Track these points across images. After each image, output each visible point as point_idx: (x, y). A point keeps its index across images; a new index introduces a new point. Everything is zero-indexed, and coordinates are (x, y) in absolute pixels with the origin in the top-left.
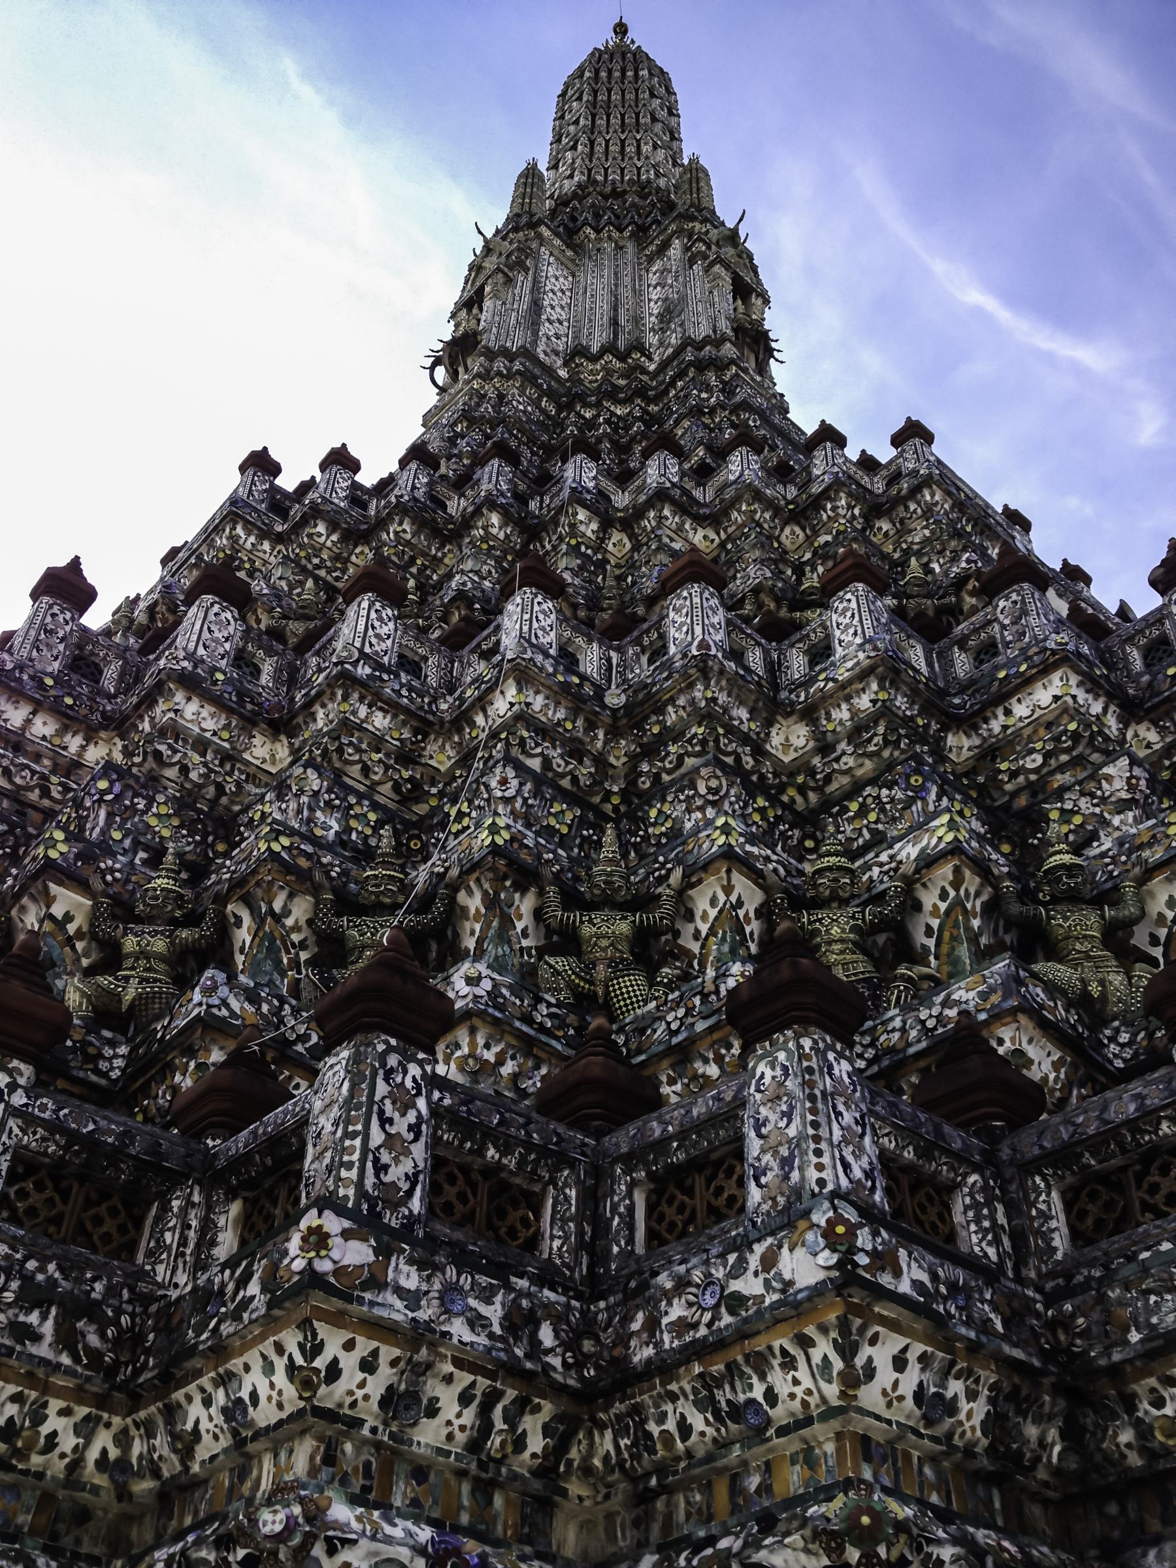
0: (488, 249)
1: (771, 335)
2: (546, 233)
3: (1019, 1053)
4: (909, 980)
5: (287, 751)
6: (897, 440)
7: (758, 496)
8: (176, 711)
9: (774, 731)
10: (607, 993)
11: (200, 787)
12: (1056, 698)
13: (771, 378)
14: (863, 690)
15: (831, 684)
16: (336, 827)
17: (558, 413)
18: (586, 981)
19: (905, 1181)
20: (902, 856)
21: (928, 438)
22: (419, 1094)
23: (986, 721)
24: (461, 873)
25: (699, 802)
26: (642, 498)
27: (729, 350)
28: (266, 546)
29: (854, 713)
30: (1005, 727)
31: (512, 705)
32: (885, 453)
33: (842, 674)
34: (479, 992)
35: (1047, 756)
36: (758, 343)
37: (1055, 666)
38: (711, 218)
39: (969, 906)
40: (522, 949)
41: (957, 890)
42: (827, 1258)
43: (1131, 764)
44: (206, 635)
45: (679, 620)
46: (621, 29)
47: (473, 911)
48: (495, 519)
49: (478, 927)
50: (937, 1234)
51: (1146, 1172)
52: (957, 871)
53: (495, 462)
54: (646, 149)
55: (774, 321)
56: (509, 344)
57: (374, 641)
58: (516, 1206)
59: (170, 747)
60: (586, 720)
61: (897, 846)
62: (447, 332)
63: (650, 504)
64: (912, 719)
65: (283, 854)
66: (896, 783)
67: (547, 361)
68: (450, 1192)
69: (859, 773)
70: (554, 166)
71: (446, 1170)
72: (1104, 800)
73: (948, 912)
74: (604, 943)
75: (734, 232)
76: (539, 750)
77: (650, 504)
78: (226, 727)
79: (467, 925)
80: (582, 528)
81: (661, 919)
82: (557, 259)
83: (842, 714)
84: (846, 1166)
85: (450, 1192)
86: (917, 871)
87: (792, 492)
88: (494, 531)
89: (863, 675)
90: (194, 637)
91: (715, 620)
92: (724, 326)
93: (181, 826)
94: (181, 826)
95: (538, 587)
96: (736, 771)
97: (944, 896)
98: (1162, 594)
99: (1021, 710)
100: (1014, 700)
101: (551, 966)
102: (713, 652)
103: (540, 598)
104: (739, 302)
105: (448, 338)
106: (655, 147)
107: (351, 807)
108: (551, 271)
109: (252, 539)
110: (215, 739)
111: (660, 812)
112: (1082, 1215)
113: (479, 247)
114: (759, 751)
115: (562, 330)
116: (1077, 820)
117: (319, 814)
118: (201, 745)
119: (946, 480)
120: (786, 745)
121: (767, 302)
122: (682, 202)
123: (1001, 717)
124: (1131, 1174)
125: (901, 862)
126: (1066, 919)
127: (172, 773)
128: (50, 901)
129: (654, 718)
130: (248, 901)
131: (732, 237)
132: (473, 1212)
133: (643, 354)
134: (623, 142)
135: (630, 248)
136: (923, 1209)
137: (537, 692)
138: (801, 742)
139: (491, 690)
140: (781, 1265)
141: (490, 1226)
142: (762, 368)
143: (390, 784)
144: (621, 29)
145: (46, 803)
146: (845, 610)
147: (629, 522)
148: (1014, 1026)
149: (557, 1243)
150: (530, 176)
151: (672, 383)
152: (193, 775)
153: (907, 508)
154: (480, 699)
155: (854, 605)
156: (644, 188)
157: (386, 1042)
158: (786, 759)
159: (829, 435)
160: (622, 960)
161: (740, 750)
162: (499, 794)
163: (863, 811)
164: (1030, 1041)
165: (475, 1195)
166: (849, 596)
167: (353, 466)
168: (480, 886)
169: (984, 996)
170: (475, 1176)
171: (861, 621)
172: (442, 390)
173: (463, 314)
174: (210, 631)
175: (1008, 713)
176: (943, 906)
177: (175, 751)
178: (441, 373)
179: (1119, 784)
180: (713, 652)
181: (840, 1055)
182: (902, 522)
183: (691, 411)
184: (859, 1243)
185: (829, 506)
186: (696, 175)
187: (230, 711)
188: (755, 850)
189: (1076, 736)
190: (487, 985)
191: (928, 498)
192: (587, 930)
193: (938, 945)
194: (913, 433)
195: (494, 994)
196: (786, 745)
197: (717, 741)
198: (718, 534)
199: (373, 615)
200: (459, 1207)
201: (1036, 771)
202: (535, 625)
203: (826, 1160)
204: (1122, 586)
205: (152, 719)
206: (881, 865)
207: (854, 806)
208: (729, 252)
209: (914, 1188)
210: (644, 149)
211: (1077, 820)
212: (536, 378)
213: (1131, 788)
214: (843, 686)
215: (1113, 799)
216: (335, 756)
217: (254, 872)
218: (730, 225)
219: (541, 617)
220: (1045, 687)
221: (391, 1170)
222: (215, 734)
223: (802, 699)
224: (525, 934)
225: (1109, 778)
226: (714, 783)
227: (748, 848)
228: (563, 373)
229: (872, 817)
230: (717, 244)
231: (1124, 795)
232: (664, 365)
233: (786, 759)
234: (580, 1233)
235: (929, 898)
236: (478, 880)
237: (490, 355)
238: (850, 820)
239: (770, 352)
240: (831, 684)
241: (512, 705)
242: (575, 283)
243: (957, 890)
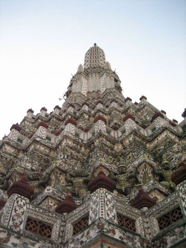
0: (73, 77)
1: (121, 87)
3: (156, 197)
4: (137, 187)
6: (141, 99)
7: (116, 109)
8: (6, 149)
9: (115, 146)
10: (78, 193)
11: (9, 162)
12: (166, 136)
13: (122, 94)
14: (131, 137)
16: (30, 166)
18: (74, 191)
19: (124, 219)
21: (146, 98)
22: (24, 205)
23: (154, 141)
24: (51, 172)
26: (96, 111)
27: (115, 90)
28: (31, 125)
30: (157, 142)
31: (65, 143)
32: (139, 101)
33: (127, 134)
34: (50, 192)
35: (165, 146)
36: (119, 89)
37: (165, 130)
38: (110, 70)
39: (148, 172)
40: (62, 186)
41: (145, 169)
42: (97, 230)
43: (178, 145)
44: (12, 136)
45: (97, 127)
46: (95, 44)
47: (53, 179)
49: (54, 182)
50: (131, 230)
51: (173, 213)
52: (145, 165)
53: (70, 107)
54: (100, 61)
55: (122, 85)
56: (77, 92)
57: (41, 134)
58: (46, 228)
59: (4, 155)
60: (80, 146)
61: (134, 162)
62: (67, 90)
63: (97, 112)
64: (140, 142)
65: (18, 170)
67: (84, 94)
68: (31, 226)
70: (85, 65)
71: (31, 221)
72: (174, 152)
73: (144, 174)
74: (77, 183)
76: (70, 151)
77: (97, 112)
78: (15, 151)
79: (52, 182)
81: (89, 178)
84: (108, 215)
85: (31, 226)
86: (138, 166)
87: (122, 109)
89: (130, 134)
90: (10, 136)
91: (103, 127)
92: (113, 86)
93: (4, 168)
94: (4, 168)
95: (71, 123)
96: (107, 152)
97: (143, 171)
98: (184, 117)
99: (160, 139)
100: (158, 137)
101: (67, 188)
102: (102, 131)
103: (71, 125)
104: (116, 82)
105: (66, 91)
106: (101, 61)
107: (33, 163)
108: (84, 80)
109: (28, 123)
110: (13, 154)
111: (91, 160)
112: (161, 224)
113: (72, 78)
114: (112, 149)
115: (86, 89)
116: (170, 156)
117: (27, 164)
118: (10, 155)
119: (149, 105)
120: (118, 148)
121: (120, 82)
122: (105, 68)
124: (170, 214)
125: (135, 165)
126: (166, 173)
129: (92, 145)
131: (114, 73)
132: (36, 230)
134: (96, 60)
136: (128, 224)
137: (70, 141)
139: (61, 141)
140: (90, 235)
141: (40, 232)
142: (120, 92)
143: (43, 160)
144: (95, 44)
146: (127, 123)
148: (154, 192)
149: (54, 236)
150: (80, 66)
151: (105, 96)
152: (8, 160)
153: (143, 110)
154: (60, 143)
155: (129, 122)
156: (100, 67)
157: (18, 196)
158: (118, 151)
159: (129, 99)
160: (81, 186)
161: (108, 149)
162: (60, 158)
163: (130, 157)
164: (158, 195)
165: (37, 226)
166: (128, 121)
167: (46, 110)
168: (54, 174)
169: (149, 187)
170: (37, 223)
172: (66, 100)
173: (69, 88)
174: (13, 135)
175: (158, 139)
176: (143, 172)
177: (5, 155)
178: (65, 97)
179: (176, 149)
180: (102, 131)
181: (109, 194)
184: (105, 227)
186: (108, 64)
187: (16, 148)
188: (107, 164)
189: (169, 142)
190: (51, 191)
191: (146, 108)
192: (74, 181)
193: (143, 180)
195: (53, 192)
197: (103, 147)
199: (41, 130)
200: (33, 229)
201: (163, 149)
202: (70, 130)
203: (103, 213)
204: (175, 114)
205: (2, 150)
206: (132, 166)
207: (128, 157)
208: (113, 75)
209: (126, 221)
210: (99, 61)
211: (170, 156)
213: (178, 149)
214: (127, 136)
215: (175, 152)
216: (32, 154)
218: (114, 71)
219: (71, 128)
220: (164, 134)
221: (16, 220)
222: (13, 152)
223: (120, 139)
224: (63, 183)
225: (174, 148)
226: (100, 154)
227: (105, 164)
228: (86, 96)
229: (131, 158)
230: (112, 74)
231: (178, 151)
232: (103, 93)
233: (118, 151)
234: (59, 234)
235: (141, 172)
236: (54, 173)
237: (73, 94)
238: (128, 159)
239: (121, 90)
240: (125, 136)
241: (65, 143)
243: (145, 169)
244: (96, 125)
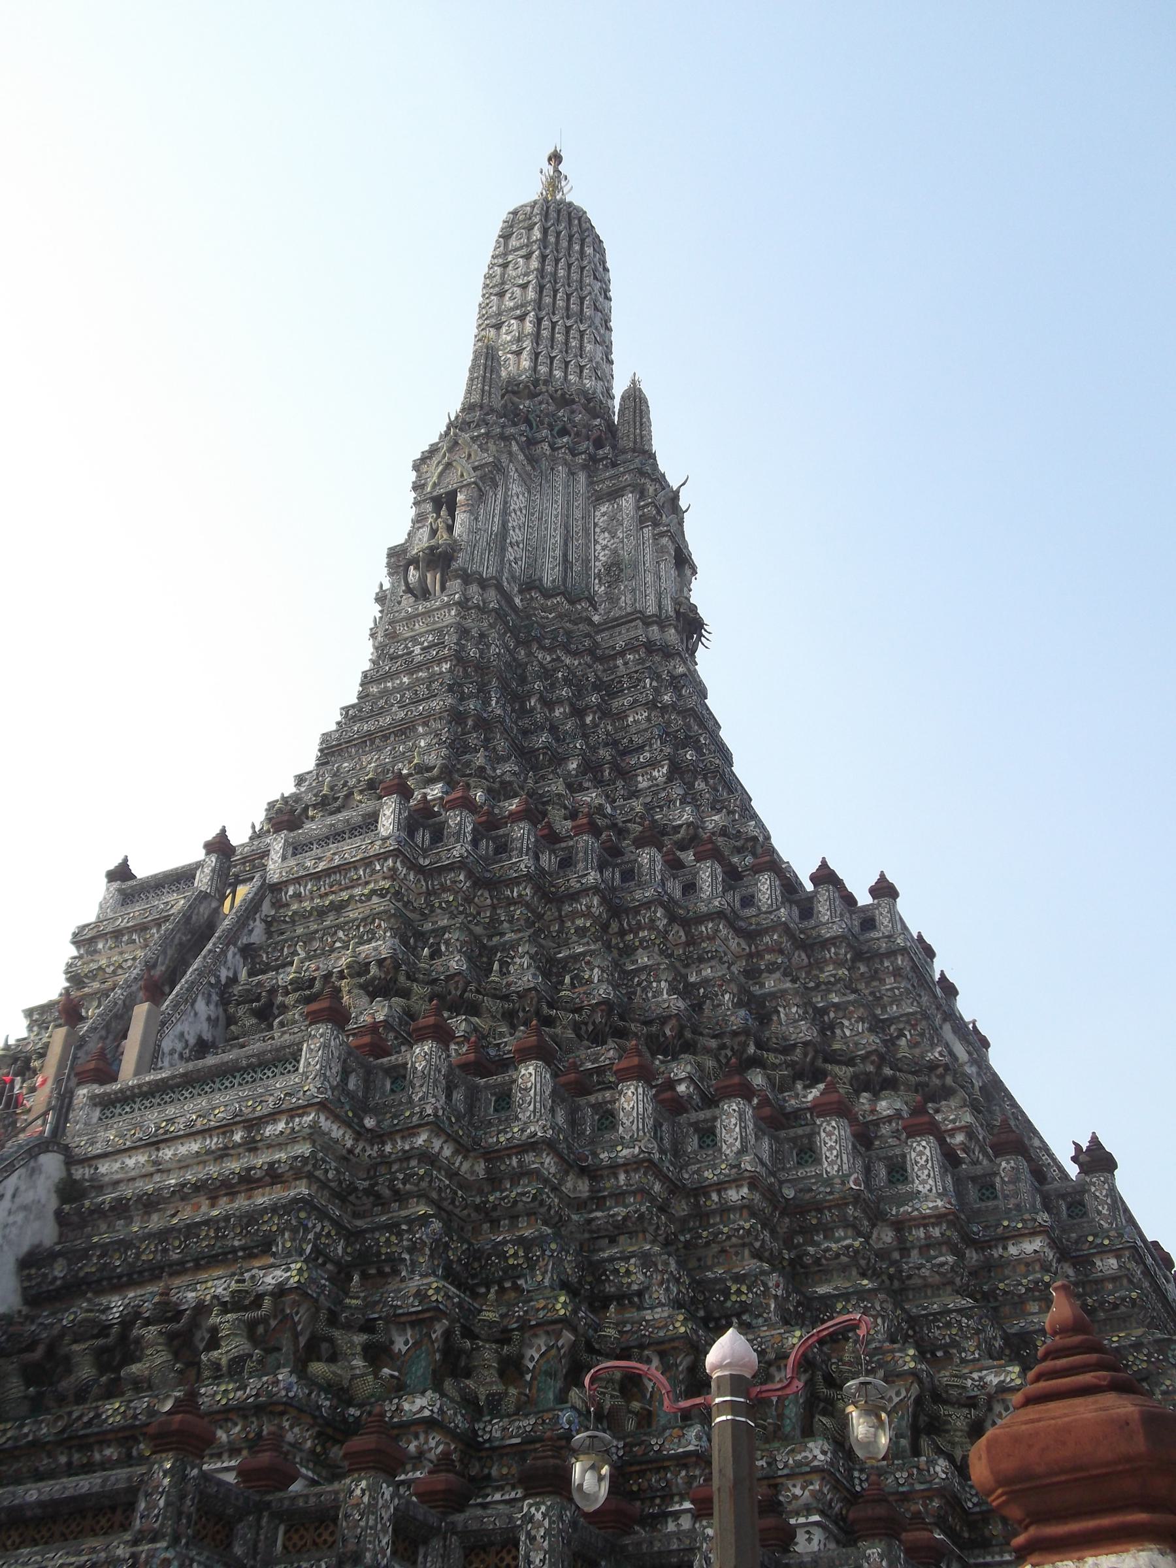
2: (515, 448)
5: (587, 1188)
6: (874, 891)
15: (916, 1213)
17: (516, 648)
20: (988, 1379)
25: (873, 1313)
29: (928, 1236)
37: (1040, 1233)
48: (596, 901)
66: (972, 1318)
69: (930, 1280)
75: (675, 496)
80: (658, 923)
82: (520, 475)
83: (921, 1233)
88: (593, 910)
111: (844, 1307)
120: (879, 1239)
121: (694, 572)
123: (1001, 1250)
127: (543, 1210)
128: (559, 1336)
129: (813, 1213)
130: (662, 1355)
133: (591, 604)
135: (582, 477)
138: (889, 1240)
144: (556, 158)
145: (451, 1207)
147: (686, 923)
152: (552, 1212)
153: (882, 963)
154: (718, 1184)
171: (933, 1167)
175: (1005, 1248)
182: (876, 972)
183: (647, 704)
185: (833, 950)
194: (884, 890)
196: (879, 1239)
198: (750, 947)
206: (973, 1379)
212: (506, 615)
217: (672, 1340)
229: (954, 1331)
237: (467, 578)
238: (939, 1328)
241: (743, 1198)
242: (529, 500)
244: (829, 1134)
